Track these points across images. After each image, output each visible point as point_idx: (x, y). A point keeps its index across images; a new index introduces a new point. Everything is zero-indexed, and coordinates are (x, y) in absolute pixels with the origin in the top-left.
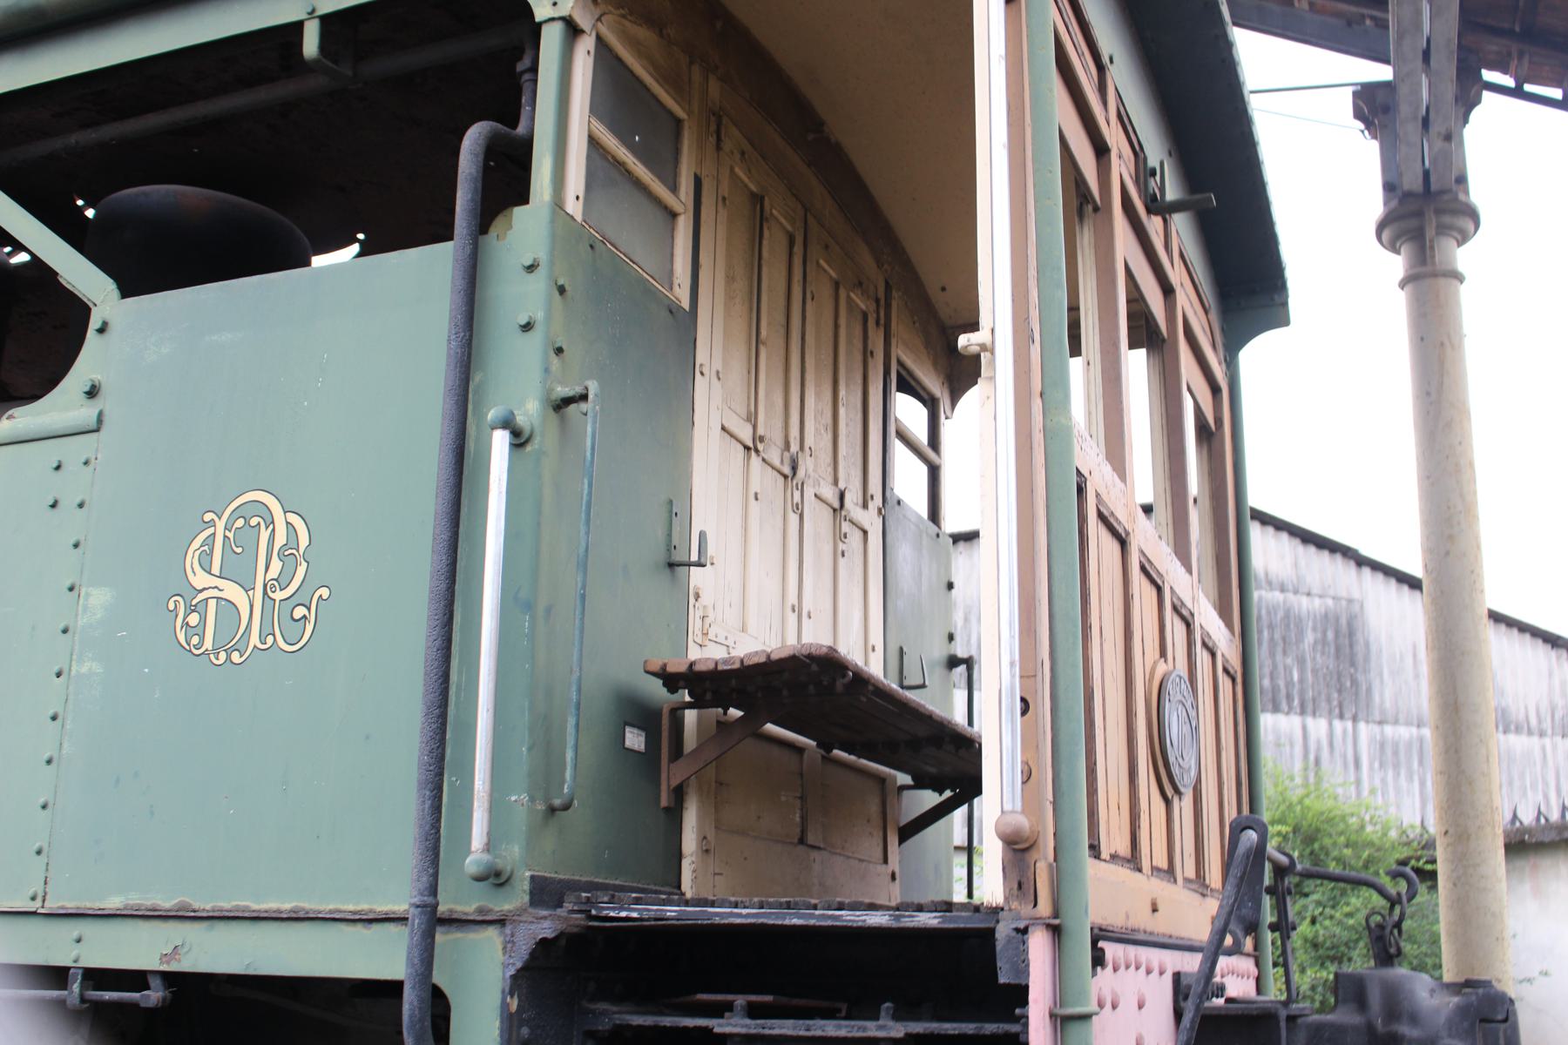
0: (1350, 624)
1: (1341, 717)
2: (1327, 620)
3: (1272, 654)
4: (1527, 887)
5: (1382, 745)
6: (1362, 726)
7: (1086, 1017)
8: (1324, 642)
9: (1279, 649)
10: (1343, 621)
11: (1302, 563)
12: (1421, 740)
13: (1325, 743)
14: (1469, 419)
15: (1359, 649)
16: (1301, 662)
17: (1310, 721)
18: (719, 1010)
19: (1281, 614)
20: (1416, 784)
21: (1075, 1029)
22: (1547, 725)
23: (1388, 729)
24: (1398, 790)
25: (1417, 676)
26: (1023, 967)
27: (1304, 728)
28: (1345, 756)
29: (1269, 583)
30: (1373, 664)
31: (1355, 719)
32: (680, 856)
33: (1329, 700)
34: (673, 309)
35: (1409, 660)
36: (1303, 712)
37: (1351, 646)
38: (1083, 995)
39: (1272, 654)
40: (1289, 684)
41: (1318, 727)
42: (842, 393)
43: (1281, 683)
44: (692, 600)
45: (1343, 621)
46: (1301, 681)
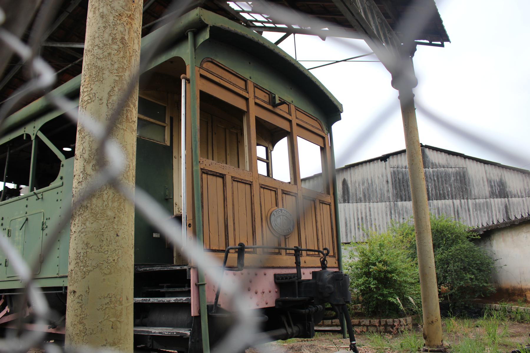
0: (464, 174)
1: (463, 199)
2: (457, 174)
3: (442, 184)
4: (501, 240)
5: (476, 205)
6: (469, 200)
7: (204, 284)
8: (457, 179)
9: (444, 183)
10: (462, 174)
11: (449, 160)
12: (487, 202)
13: (459, 206)
14: (417, 130)
15: (467, 180)
16: (451, 185)
17: (454, 201)
18: (162, 287)
19: (444, 174)
20: (486, 214)
21: (201, 287)
22: (524, 194)
23: (477, 201)
24: (481, 216)
25: (484, 186)
26: (190, 276)
27: (453, 203)
28: (465, 209)
29: (440, 166)
30: (471, 184)
31: (467, 199)
32: (173, 257)
33: (460, 195)
34: (166, 147)
35: (481, 182)
36: (452, 199)
37: (465, 180)
38: (202, 281)
39: (442, 184)
40: (448, 192)
41: (457, 202)
42: (228, 152)
43: (446, 192)
44: (174, 205)
45: (462, 174)
46: (451, 190)
